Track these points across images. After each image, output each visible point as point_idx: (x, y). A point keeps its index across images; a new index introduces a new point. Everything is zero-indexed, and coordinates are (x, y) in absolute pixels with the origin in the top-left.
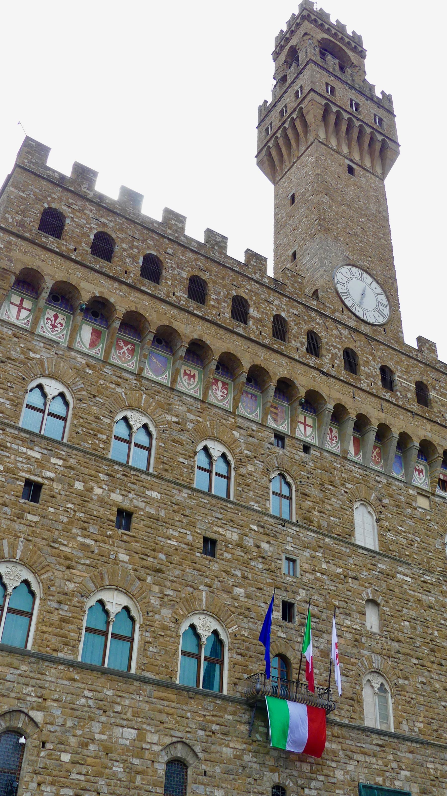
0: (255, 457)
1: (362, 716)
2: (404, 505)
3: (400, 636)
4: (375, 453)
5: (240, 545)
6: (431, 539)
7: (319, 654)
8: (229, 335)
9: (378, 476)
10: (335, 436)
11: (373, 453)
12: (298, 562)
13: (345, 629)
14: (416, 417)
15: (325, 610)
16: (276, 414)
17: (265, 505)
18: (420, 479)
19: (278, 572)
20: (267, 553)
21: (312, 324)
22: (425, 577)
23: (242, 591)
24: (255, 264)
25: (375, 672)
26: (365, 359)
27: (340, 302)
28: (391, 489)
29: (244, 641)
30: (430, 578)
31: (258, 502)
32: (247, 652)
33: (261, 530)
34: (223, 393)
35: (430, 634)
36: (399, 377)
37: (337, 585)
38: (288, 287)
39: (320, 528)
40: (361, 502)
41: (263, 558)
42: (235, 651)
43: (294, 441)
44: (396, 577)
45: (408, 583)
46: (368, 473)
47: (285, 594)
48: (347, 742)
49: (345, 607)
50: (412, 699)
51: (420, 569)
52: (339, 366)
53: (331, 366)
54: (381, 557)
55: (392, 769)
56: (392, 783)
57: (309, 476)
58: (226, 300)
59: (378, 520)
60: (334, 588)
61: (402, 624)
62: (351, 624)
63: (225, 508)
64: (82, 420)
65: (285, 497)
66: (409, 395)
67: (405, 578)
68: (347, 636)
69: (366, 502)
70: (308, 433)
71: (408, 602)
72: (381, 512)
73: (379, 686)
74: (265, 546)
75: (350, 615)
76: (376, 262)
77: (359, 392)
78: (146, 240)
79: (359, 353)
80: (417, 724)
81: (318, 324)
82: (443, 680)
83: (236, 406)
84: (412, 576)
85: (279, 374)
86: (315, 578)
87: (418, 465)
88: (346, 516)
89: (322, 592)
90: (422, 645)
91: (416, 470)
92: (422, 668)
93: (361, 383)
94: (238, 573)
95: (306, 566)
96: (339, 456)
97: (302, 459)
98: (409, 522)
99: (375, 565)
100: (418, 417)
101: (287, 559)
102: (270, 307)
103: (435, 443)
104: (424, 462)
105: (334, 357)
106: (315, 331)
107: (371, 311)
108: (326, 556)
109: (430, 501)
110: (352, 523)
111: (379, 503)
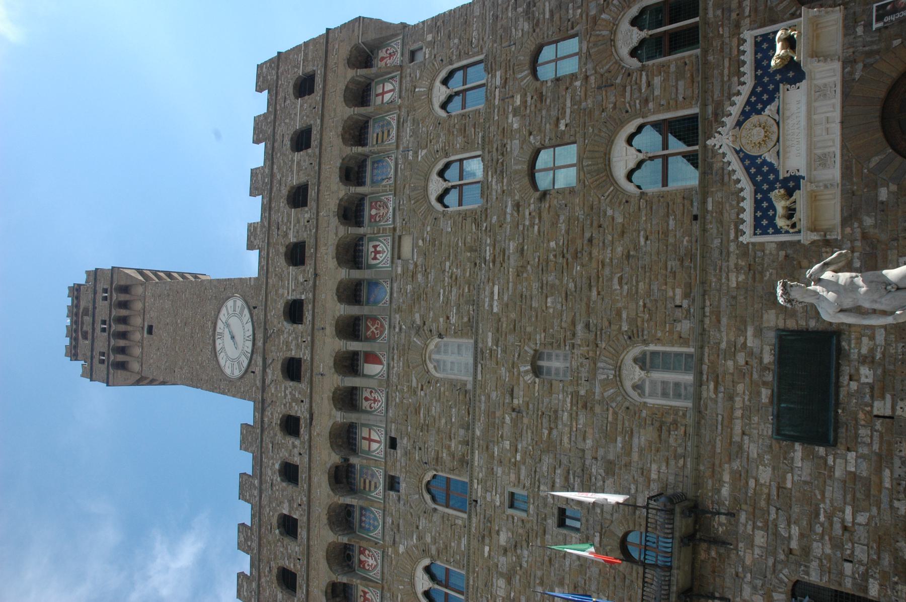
1: (681, 413)
3: (567, 318)
5: (509, 581)
9: (394, 328)
19: (528, 526)
25: (620, 376)
31: (460, 538)
33: (487, 541)
35: (555, 256)
41: (516, 546)
44: (497, 314)
47: (549, 521)
48: (718, 450)
50: (645, 306)
54: (480, 340)
55: (747, 363)
56: (766, 368)
59: (440, 336)
60: (529, 434)
67: (496, 297)
70: (377, 438)
74: (503, 539)
75: (556, 412)
80: (678, 303)
88: (447, 393)
95: (513, 477)
98: (431, 277)
108: (496, 439)
110: (452, 384)
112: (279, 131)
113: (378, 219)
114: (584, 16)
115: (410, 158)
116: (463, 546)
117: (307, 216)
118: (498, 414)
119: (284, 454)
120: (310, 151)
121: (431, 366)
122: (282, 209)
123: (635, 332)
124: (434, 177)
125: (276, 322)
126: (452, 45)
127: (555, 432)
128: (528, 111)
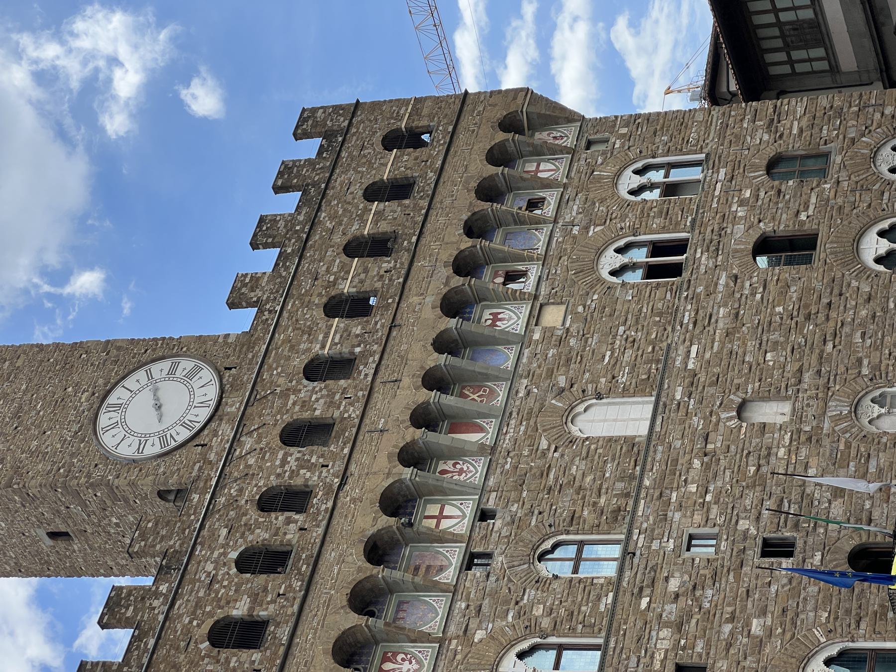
0: (517, 603)
2: (564, 350)
4: (475, 397)
5: (679, 627)
6: (619, 307)
7: (840, 500)
8: (296, 651)
9: (517, 392)
10: (454, 465)
11: (473, 399)
12: (692, 531)
13: (794, 457)
14: (397, 322)
15: (767, 489)
16: (428, 568)
17: (602, 585)
18: (510, 318)
20: (685, 582)
21: (243, 502)
22: (686, 321)
23: (755, 622)
24: (131, 608)
25: (855, 412)
26: (297, 408)
27: (184, 450)
28: (538, 371)
29: (836, 618)
30: (687, 314)
31: (599, 598)
32: (854, 613)
33: (647, 591)
34: (403, 660)
35: (782, 318)
36: (323, 347)
37: (722, 468)
38: (171, 547)
39: (627, 495)
40: (570, 424)
42: (853, 632)
43: (475, 535)
44: (694, 370)
45: (701, 350)
46: (515, 410)
47: (750, 552)
49: (756, 456)
51: (673, 329)
52: (322, 456)
53: (325, 470)
54: (663, 394)
57: (536, 512)
58: (222, 660)
59: (599, 397)
60: (728, 473)
61: (771, 363)
62: (784, 447)
63: (618, 651)
65: (580, 551)
66: (358, 330)
67: (693, 354)
68: (804, 454)
69: (569, 414)
71: (734, 353)
72: (584, 391)
73: (877, 406)
74: (674, 585)
76: (76, 378)
77: (367, 421)
79: (287, 418)
81: (241, 491)
82: (854, 303)
83: (426, 638)
84: (687, 343)
85: (360, 563)
86: (715, 503)
87: (483, 320)
88: (600, 451)
89: (737, 492)
90: (801, 333)
91: (494, 325)
92: (839, 336)
93: (350, 416)
94: (727, 628)
95: (697, 518)
96: (490, 460)
97: (508, 524)
98: (593, 341)
99: (679, 404)
100: (399, 316)
101: (688, 550)
102: (223, 580)
103: (444, 291)
104: (477, 310)
105: (303, 464)
106: (257, 497)
107: (192, 392)
108: (675, 485)
109: (547, 304)
114: (841, 137)
116: (602, 608)
120: (406, 202)
122: (327, 259)
123: (877, 373)
127: (764, 469)
128: (760, 203)
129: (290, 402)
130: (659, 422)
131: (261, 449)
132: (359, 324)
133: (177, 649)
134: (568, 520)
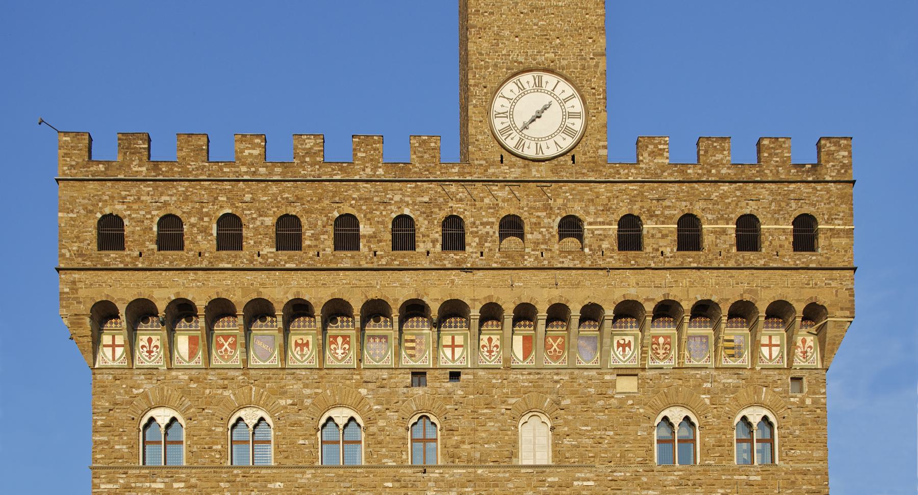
21: (450, 205)
36: (590, 224)
38: (414, 166)
59: (552, 429)
64: (195, 438)
78: (216, 198)
88: (506, 438)
98: (601, 416)
106: (455, 214)
110: (515, 443)
111: (557, 407)
112: (763, 192)
113: (654, 346)
115: (705, 385)
116: (384, 461)
117: (667, 251)
118: (497, 489)
119: (422, 224)
120: (734, 250)
121: (526, 418)
124: (686, 413)
125: (560, 201)
126: (795, 427)
129: (539, 214)
130: (530, 470)
131: (497, 205)
132: (612, 245)
133: (333, 197)
134: (450, 428)
